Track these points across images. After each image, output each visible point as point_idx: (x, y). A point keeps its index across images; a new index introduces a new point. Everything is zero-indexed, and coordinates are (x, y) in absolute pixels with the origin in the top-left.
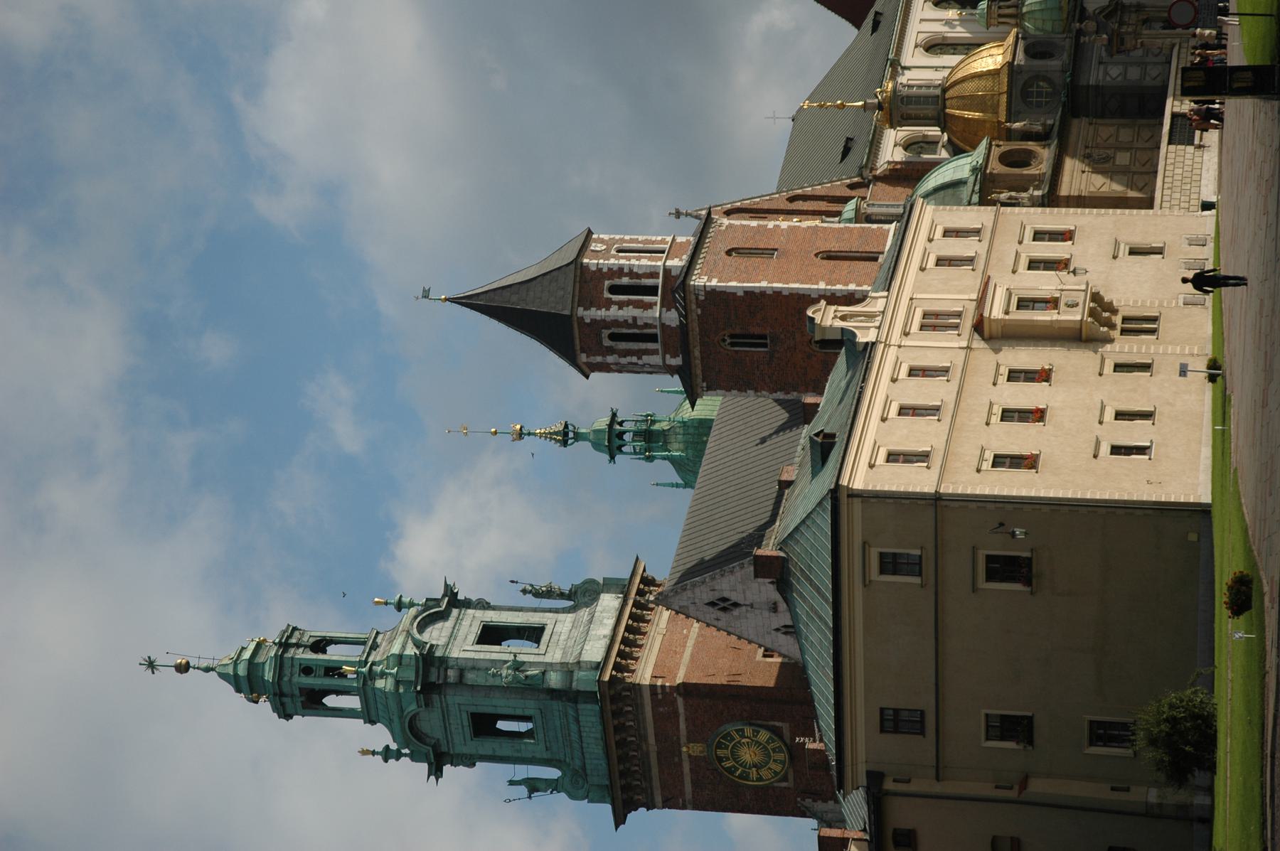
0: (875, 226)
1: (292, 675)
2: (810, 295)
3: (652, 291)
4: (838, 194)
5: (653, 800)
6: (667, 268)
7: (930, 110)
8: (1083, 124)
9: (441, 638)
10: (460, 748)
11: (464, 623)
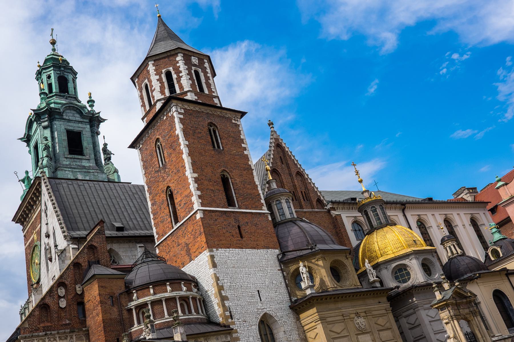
0: (263, 201)
1: (46, 72)
2: (186, 171)
4: (311, 195)
5: (25, 230)
6: (189, 94)
7: (375, 223)
8: (384, 305)
9: (68, 117)
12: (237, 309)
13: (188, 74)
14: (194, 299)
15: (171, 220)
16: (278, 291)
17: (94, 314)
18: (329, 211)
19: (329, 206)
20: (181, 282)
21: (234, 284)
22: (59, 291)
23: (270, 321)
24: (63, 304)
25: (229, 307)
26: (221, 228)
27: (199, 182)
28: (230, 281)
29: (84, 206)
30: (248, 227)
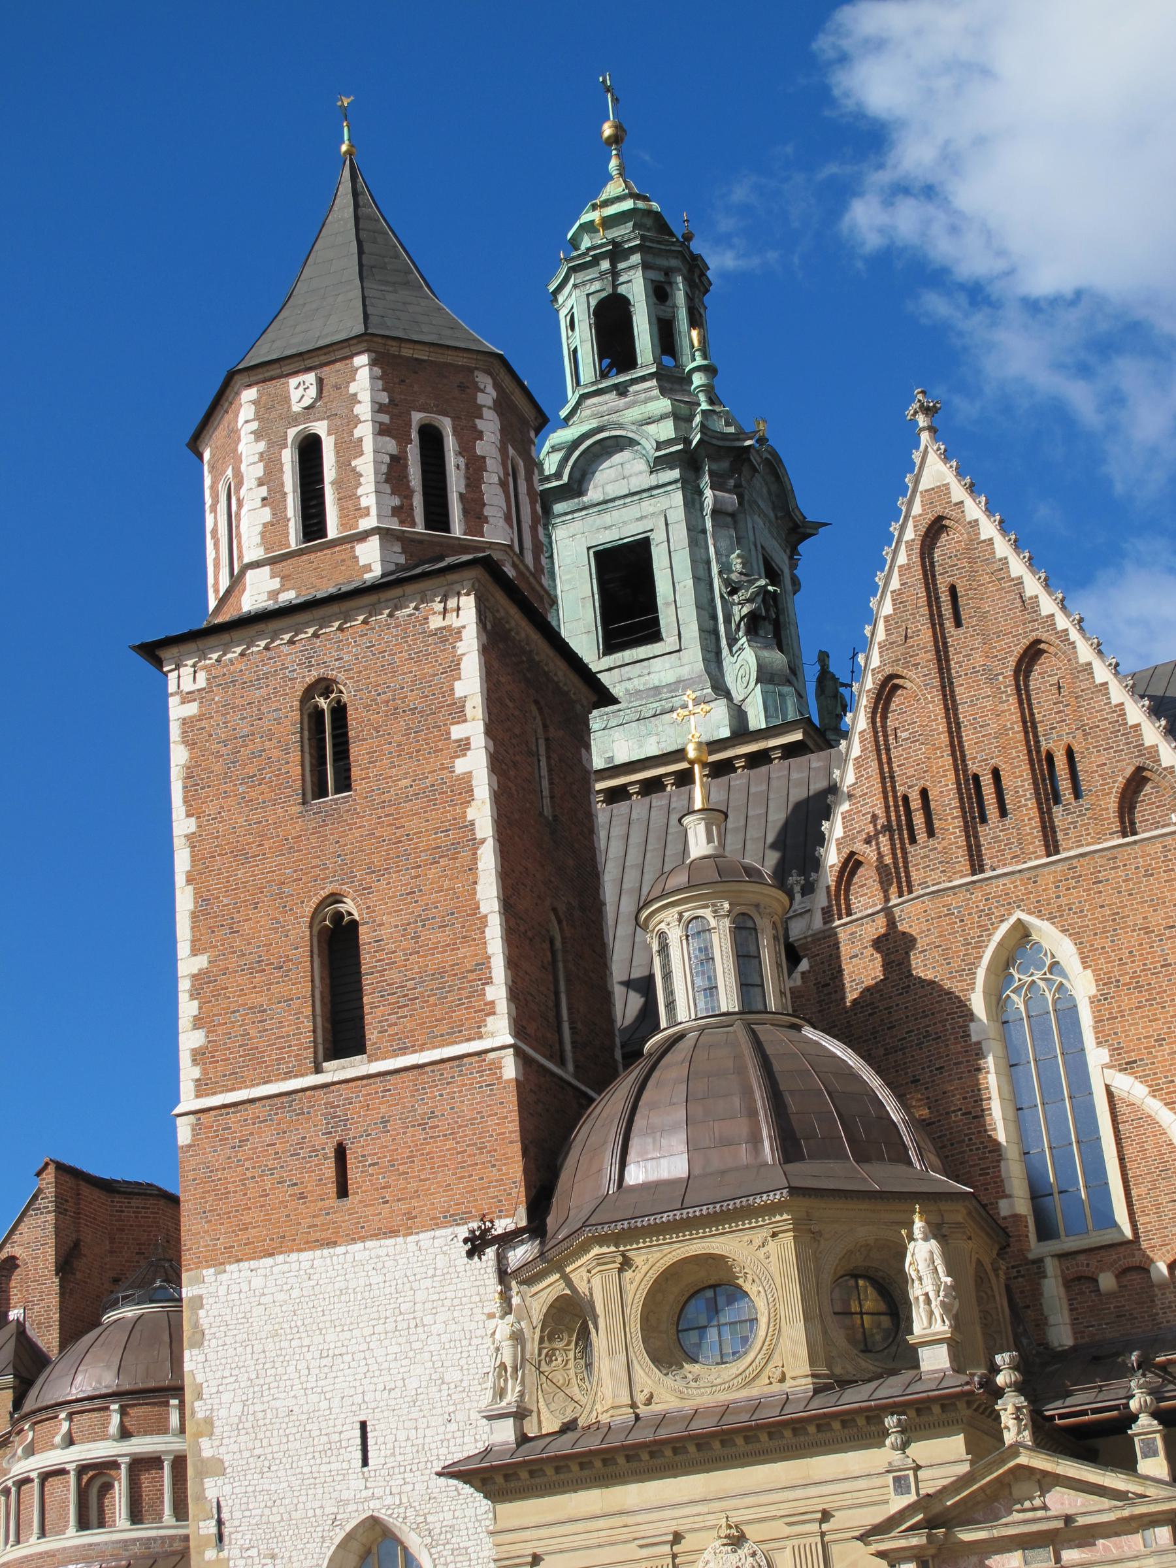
0: (498, 992)
11: (644, 504)
12: (251, 1507)
13: (260, 484)
16: (460, 1416)
20: (107, 1408)
21: (258, 1407)
25: (218, 1503)
27: (207, 991)
28: (244, 1397)
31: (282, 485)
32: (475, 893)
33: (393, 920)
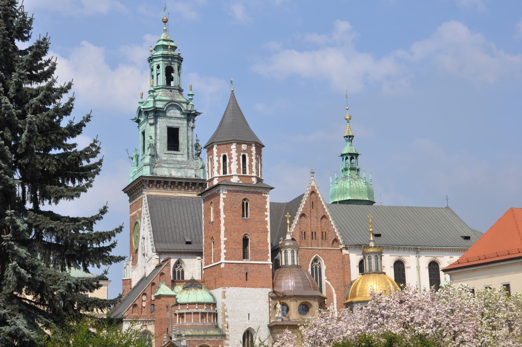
1: (156, 62)
3: (225, 172)
6: (234, 177)
10: (140, 128)
11: (179, 121)
13: (236, 161)
14: (210, 314)
15: (212, 258)
17: (158, 314)
18: (341, 250)
19: (343, 246)
21: (234, 309)
22: (143, 297)
23: (252, 332)
24: (144, 304)
26: (234, 274)
27: (227, 244)
29: (168, 222)
30: (253, 273)
31: (240, 162)
32: (267, 239)
33: (255, 240)
